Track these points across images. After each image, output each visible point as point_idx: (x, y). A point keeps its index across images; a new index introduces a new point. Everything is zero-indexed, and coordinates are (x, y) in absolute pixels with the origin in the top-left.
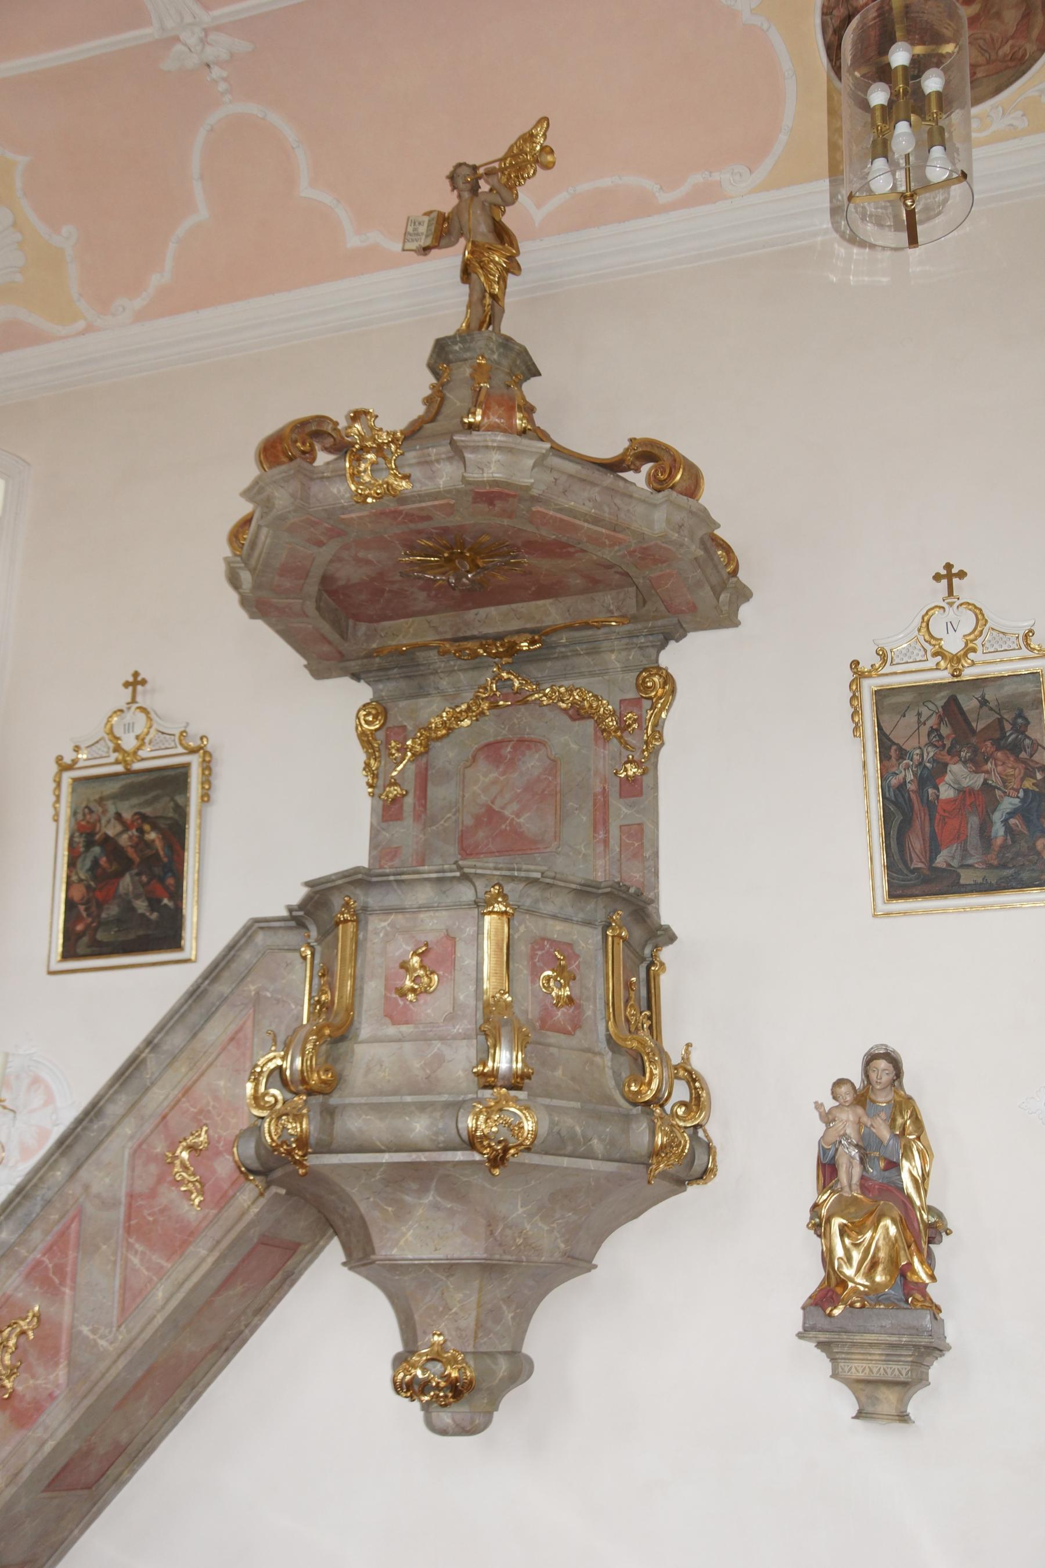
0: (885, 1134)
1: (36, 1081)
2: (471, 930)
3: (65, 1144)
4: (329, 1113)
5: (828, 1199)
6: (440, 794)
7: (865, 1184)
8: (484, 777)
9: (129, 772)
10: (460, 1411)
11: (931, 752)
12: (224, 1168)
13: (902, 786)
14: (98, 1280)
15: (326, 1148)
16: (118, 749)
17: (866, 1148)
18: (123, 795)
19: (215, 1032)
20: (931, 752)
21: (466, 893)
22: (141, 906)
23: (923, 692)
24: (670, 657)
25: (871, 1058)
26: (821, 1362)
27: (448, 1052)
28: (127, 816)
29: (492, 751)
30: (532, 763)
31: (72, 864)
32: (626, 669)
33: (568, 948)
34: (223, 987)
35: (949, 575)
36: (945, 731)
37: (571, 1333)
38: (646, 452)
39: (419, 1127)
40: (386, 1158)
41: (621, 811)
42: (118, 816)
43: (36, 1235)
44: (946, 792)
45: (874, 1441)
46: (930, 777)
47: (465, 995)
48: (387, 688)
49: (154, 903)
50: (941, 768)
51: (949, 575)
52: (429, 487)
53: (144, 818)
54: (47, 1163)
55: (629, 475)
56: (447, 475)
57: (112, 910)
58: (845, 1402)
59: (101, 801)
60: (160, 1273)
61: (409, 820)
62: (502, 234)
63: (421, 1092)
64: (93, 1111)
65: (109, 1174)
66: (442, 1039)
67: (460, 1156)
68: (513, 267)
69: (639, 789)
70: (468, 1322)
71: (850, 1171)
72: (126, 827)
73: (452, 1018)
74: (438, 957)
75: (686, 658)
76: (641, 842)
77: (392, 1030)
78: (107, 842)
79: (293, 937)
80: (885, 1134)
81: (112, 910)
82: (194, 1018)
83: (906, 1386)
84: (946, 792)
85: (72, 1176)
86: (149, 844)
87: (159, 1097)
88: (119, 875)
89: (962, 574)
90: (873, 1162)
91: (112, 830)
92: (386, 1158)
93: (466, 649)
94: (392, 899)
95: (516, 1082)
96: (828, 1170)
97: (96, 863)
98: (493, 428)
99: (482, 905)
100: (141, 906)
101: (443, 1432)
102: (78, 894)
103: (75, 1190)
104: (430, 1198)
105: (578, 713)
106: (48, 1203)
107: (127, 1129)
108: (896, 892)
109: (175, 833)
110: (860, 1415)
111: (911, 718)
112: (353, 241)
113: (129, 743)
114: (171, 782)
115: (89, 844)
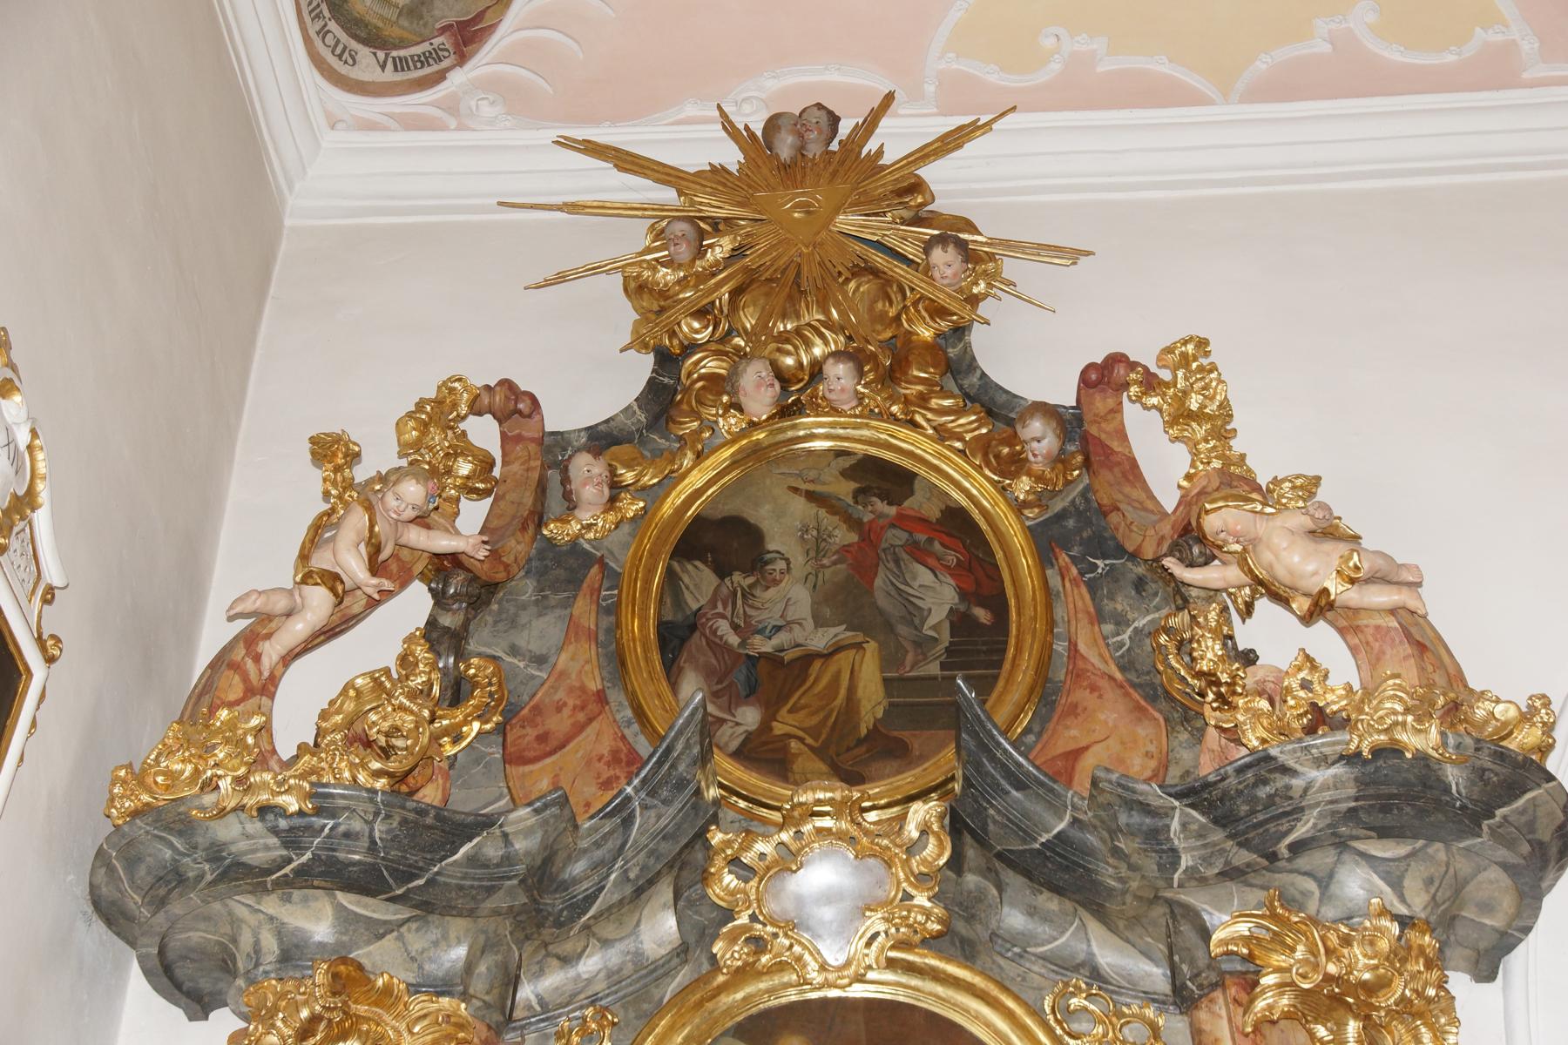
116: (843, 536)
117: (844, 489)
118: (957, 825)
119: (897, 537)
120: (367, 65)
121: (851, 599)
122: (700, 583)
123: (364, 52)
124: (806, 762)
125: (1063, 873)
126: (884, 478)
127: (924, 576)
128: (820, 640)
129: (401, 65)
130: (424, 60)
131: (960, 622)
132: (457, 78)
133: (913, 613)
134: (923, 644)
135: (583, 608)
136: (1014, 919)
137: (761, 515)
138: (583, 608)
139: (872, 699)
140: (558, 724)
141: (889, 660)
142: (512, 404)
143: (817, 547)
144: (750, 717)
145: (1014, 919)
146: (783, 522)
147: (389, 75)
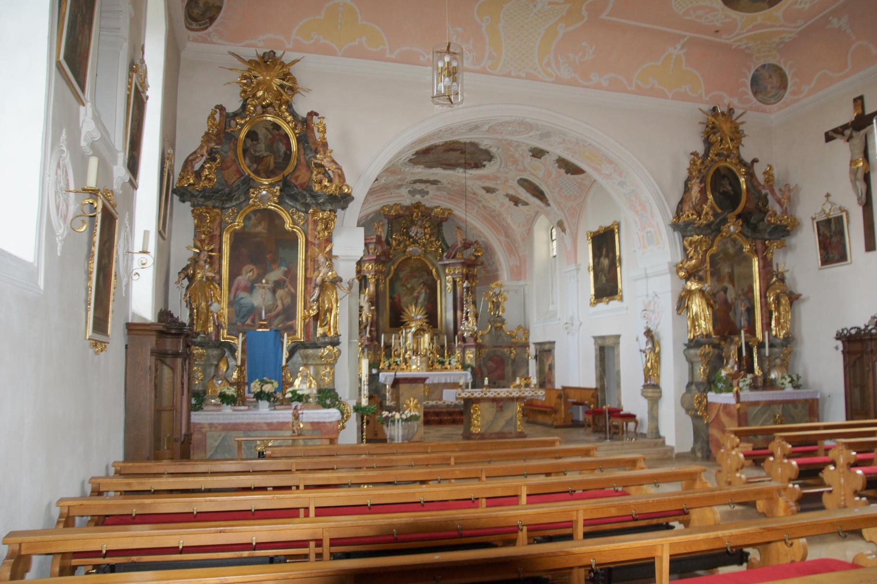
116: (270, 136)
117: (271, 128)
118: (281, 190)
119: (277, 137)
120: (195, 26)
121: (270, 147)
122: (249, 142)
123: (194, 23)
124: (262, 174)
125: (294, 198)
126: (277, 127)
127: (281, 145)
128: (265, 154)
129: (200, 25)
130: (204, 24)
131: (285, 153)
132: (210, 29)
133: (279, 151)
134: (280, 156)
135: (232, 144)
136: (287, 201)
137: (258, 131)
138: (232, 144)
139: (272, 165)
140: (229, 164)
141: (275, 159)
142: (221, 108)
143: (266, 138)
144: (255, 166)
145: (287, 201)
146: (262, 133)
147: (198, 27)
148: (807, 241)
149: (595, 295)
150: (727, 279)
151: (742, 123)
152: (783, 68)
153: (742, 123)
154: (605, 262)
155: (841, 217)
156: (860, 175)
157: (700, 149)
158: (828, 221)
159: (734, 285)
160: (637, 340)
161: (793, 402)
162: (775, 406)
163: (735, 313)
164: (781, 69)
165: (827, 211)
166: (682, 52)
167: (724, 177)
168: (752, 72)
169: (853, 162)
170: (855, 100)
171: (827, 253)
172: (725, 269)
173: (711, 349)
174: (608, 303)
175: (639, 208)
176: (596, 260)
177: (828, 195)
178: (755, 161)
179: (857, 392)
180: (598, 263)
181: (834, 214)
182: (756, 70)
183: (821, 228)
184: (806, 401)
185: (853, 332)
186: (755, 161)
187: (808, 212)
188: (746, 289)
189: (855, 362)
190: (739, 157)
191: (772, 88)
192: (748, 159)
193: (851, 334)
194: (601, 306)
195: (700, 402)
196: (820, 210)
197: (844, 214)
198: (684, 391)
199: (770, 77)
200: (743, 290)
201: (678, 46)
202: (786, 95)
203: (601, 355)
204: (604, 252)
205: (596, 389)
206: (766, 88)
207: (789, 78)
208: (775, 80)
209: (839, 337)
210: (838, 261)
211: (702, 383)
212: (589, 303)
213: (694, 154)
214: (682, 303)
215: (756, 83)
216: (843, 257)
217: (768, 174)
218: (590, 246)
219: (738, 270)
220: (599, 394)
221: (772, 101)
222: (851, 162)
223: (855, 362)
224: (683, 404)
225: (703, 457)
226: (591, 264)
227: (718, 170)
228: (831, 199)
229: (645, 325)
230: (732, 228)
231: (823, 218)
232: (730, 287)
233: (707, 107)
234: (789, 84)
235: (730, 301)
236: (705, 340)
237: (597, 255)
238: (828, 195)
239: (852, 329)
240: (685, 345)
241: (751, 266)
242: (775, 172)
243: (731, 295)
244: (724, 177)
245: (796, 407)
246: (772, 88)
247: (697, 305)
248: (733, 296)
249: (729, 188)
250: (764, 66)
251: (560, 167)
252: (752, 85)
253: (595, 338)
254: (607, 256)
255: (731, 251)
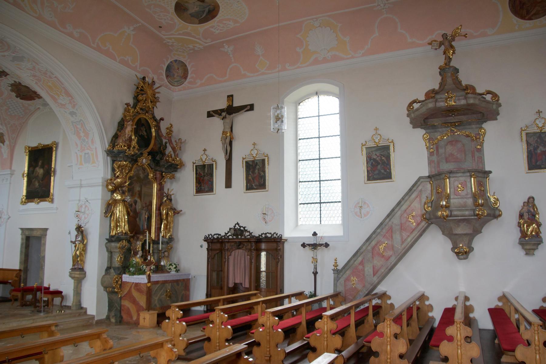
0: (532, 210)
1: (365, 203)
2: (469, 180)
3: (388, 216)
4: (451, 211)
5: (522, 221)
6: (441, 151)
7: (529, 219)
8: (449, 149)
9: (378, 146)
10: (465, 256)
11: (536, 144)
12: (419, 219)
13: (531, 150)
14: (397, 237)
15: (451, 216)
16: (375, 142)
17: (529, 212)
18: (376, 150)
19: (413, 196)
20: (536, 144)
21: (468, 174)
22: (383, 171)
23: (535, 134)
24: (484, 126)
25: (529, 198)
26: (520, 247)
27: (468, 201)
28: (378, 154)
29: (451, 143)
30: (459, 145)
31: (367, 163)
32: (476, 128)
33: (481, 182)
34: (415, 188)
35: (539, 112)
36: (539, 140)
37: (479, 243)
38: (489, 92)
39: (467, 213)
40: (460, 218)
41: (477, 154)
42: (376, 155)
43: (384, 231)
44: (539, 151)
45: (529, 259)
46: (536, 149)
47: (469, 191)
48: (428, 131)
49: (385, 171)
50: (538, 147)
51: (539, 112)
52: (460, 104)
53: (381, 155)
54: (385, 219)
55: (484, 96)
56: (463, 102)
57: (377, 172)
58: (523, 253)
59: (372, 152)
60: (409, 236)
61: (435, 155)
62: (452, 47)
63: (463, 207)
64: (393, 210)
65: (396, 220)
66: (466, 198)
67: (473, 217)
68: (454, 53)
69: (481, 151)
70: (467, 242)
71: (526, 216)
72: (378, 157)
73: (467, 195)
74: (464, 185)
75: (489, 127)
76: (481, 159)
77: (456, 197)
78: (374, 160)
79: (429, 180)
80: (532, 210)
81: (377, 172)
82: (410, 194)
83: (534, 249)
84: (539, 151)
85: (390, 220)
86: (383, 160)
87: (404, 207)
88: (377, 165)
89: (541, 112)
90: (529, 214)
91: (375, 157)
92: (460, 218)
93: (446, 124)
94: (454, 175)
95: (482, 205)
96: (521, 216)
97: (372, 163)
98: (471, 94)
99: (471, 176)
100: (383, 171)
101: (461, 259)
102: (369, 169)
103: (390, 223)
104: (464, 223)
105: (467, 136)
106: (386, 225)
107: (399, 213)
108: (529, 169)
109: (388, 157)
110: (527, 254)
111: (532, 138)
112: (409, 40)
113: (377, 141)
114: (387, 148)
115: (370, 160)
148: (187, 178)
149: (26, 196)
150: (137, 195)
151: (159, 93)
152: (187, 66)
153: (159, 93)
154: (40, 171)
155: (213, 165)
156: (228, 141)
157: (131, 102)
158: (204, 166)
159: (141, 200)
160: (70, 233)
161: (177, 281)
162: (167, 284)
163: (140, 219)
164: (186, 66)
165: (204, 160)
166: (133, 33)
167: (143, 125)
168: (168, 63)
169: (224, 133)
170: (228, 96)
171: (201, 186)
172: (137, 189)
173: (127, 244)
174: (38, 203)
175: (82, 134)
176: (31, 169)
177: (205, 150)
178: (162, 119)
179: (215, 275)
180: (33, 172)
181: (208, 162)
182: (171, 62)
183: (198, 169)
184: (184, 280)
185: (215, 237)
186: (162, 119)
187: (190, 158)
188: (148, 204)
189: (215, 255)
190: (153, 114)
191: (178, 76)
192: (158, 118)
193: (214, 238)
194: (32, 205)
195: (117, 282)
196: (199, 158)
197: (214, 163)
198: (104, 273)
199: (178, 69)
200: (146, 204)
201: (132, 28)
202: (186, 83)
203: (26, 244)
204: (40, 164)
205: (20, 270)
206: (174, 75)
207: (189, 73)
208: (180, 72)
209: (206, 239)
210: (207, 192)
211: (118, 268)
212: (20, 201)
213: (128, 105)
214: (109, 209)
215: (169, 69)
216: (210, 189)
217: (170, 130)
218: (27, 158)
219: (144, 190)
220: (22, 274)
221: (176, 84)
222: (223, 132)
223: (215, 255)
224: (102, 284)
225: (116, 322)
226: (26, 172)
227: (140, 120)
228: (207, 153)
229: (77, 222)
230: (144, 161)
231: (201, 163)
232: (138, 200)
233: (141, 76)
234: (189, 76)
235: (137, 211)
236: (123, 237)
237: (32, 164)
238: (205, 150)
239: (215, 235)
240: (107, 239)
241: (152, 188)
242: (174, 129)
243: (139, 207)
244: (143, 125)
245: (178, 285)
246: (178, 76)
247: (120, 211)
248: (140, 207)
249: (145, 134)
250: (176, 61)
251: (12, 91)
252: (166, 71)
253: (22, 229)
254: (42, 166)
255: (142, 176)
